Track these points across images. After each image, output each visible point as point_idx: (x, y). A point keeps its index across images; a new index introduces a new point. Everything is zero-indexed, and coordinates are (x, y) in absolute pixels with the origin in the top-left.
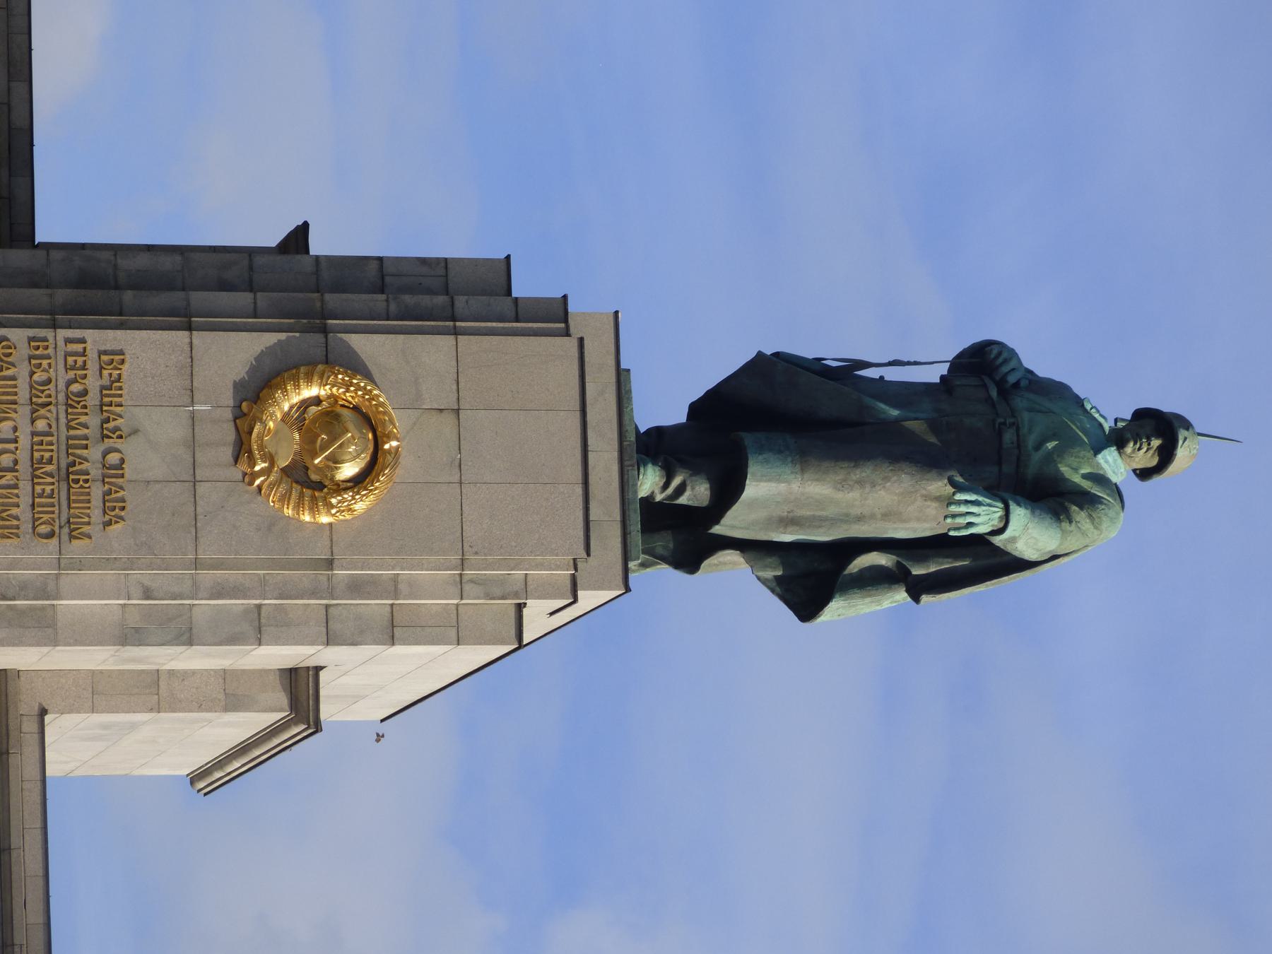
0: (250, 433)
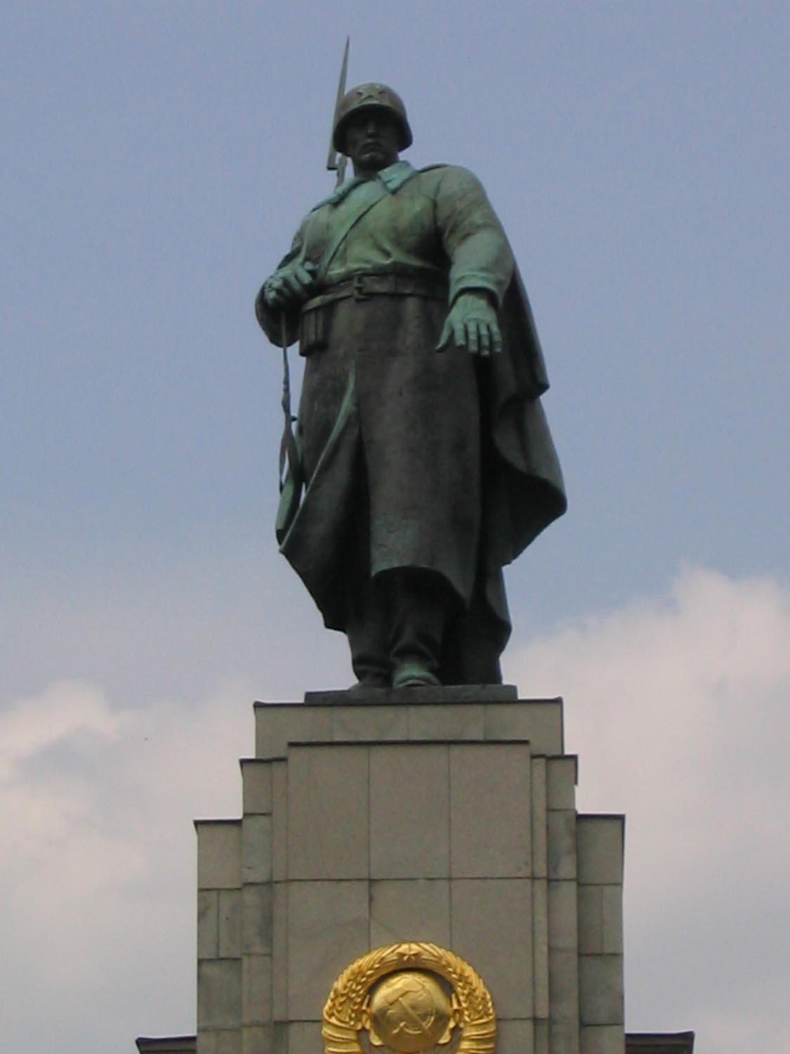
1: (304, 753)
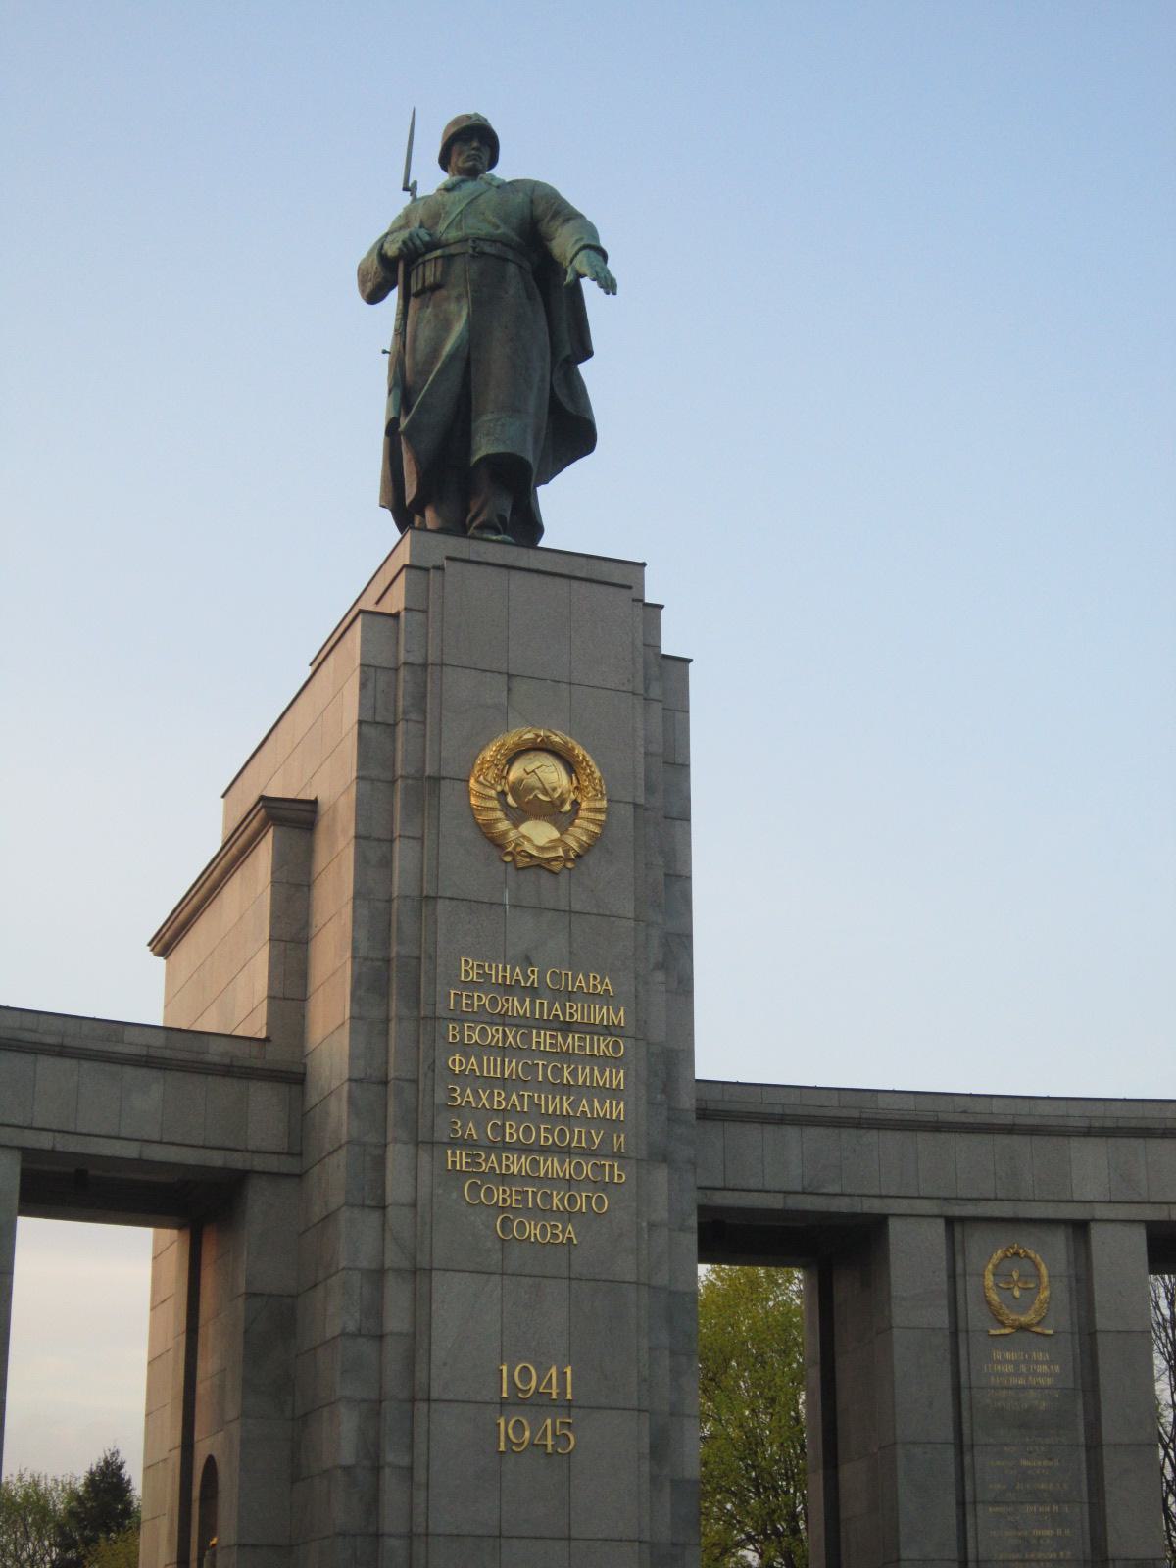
0: (531, 856)
1: (458, 565)
